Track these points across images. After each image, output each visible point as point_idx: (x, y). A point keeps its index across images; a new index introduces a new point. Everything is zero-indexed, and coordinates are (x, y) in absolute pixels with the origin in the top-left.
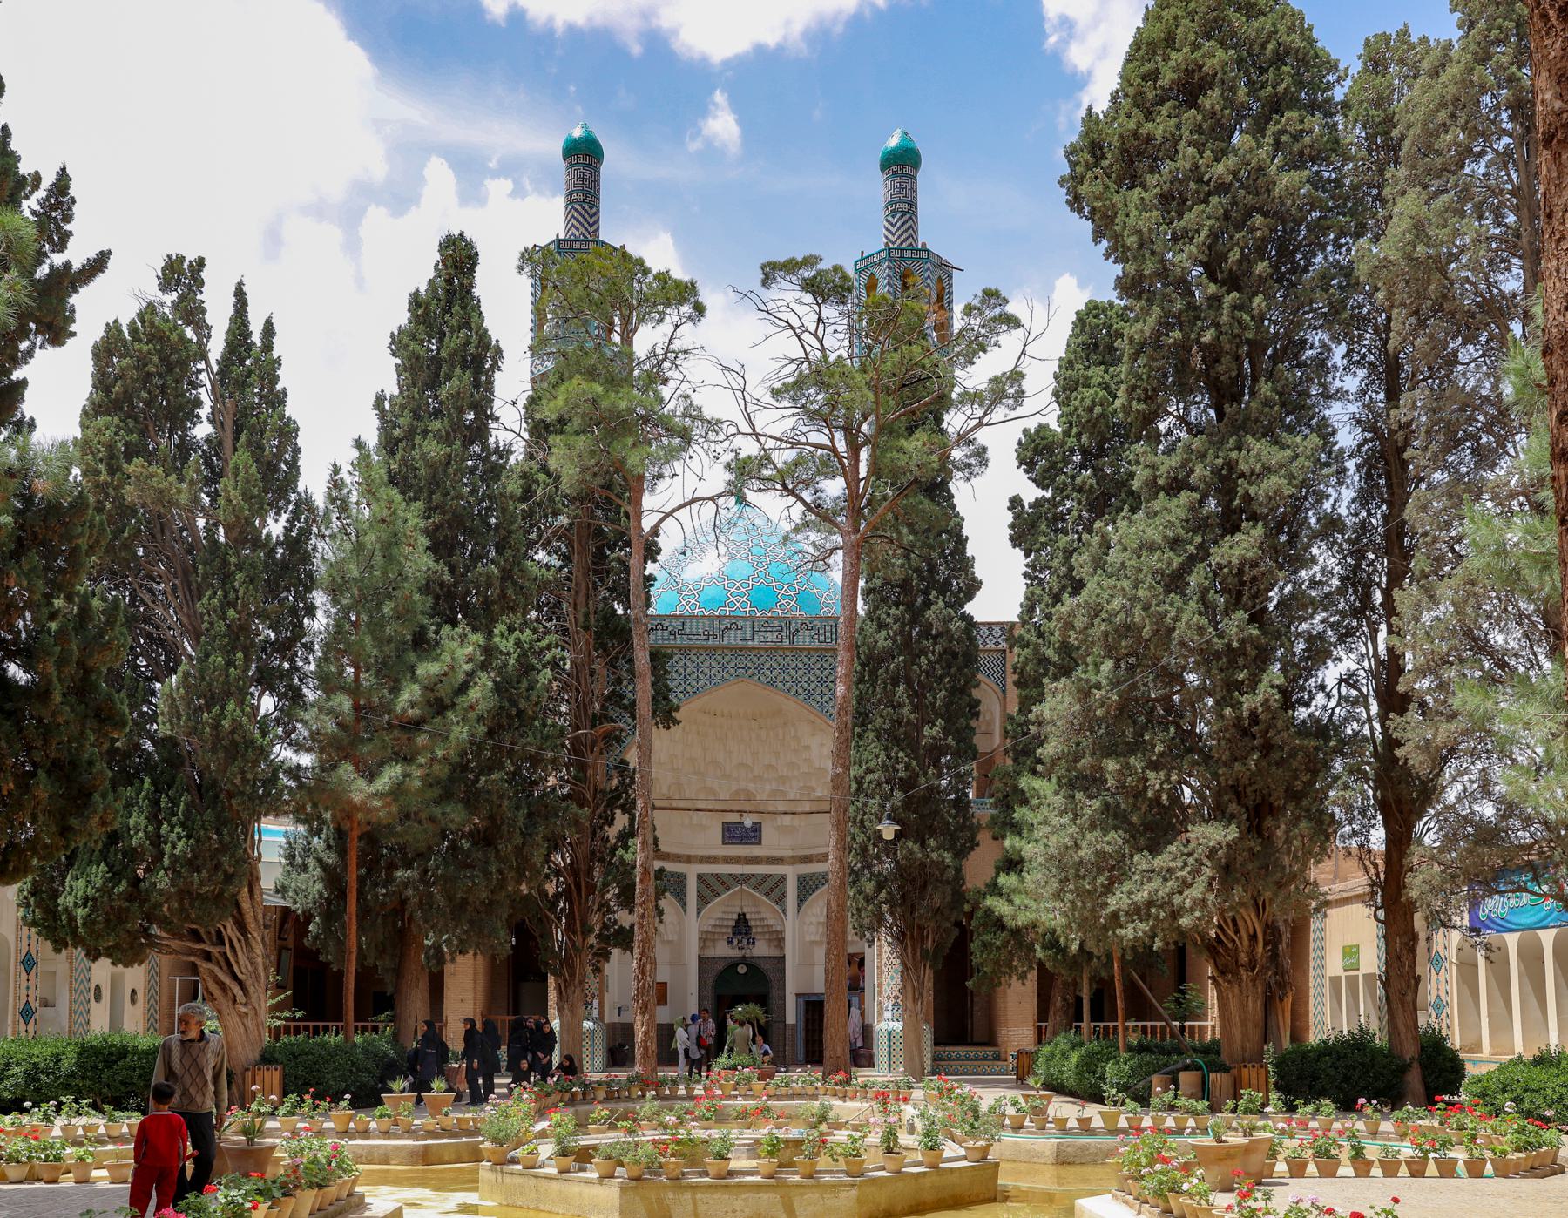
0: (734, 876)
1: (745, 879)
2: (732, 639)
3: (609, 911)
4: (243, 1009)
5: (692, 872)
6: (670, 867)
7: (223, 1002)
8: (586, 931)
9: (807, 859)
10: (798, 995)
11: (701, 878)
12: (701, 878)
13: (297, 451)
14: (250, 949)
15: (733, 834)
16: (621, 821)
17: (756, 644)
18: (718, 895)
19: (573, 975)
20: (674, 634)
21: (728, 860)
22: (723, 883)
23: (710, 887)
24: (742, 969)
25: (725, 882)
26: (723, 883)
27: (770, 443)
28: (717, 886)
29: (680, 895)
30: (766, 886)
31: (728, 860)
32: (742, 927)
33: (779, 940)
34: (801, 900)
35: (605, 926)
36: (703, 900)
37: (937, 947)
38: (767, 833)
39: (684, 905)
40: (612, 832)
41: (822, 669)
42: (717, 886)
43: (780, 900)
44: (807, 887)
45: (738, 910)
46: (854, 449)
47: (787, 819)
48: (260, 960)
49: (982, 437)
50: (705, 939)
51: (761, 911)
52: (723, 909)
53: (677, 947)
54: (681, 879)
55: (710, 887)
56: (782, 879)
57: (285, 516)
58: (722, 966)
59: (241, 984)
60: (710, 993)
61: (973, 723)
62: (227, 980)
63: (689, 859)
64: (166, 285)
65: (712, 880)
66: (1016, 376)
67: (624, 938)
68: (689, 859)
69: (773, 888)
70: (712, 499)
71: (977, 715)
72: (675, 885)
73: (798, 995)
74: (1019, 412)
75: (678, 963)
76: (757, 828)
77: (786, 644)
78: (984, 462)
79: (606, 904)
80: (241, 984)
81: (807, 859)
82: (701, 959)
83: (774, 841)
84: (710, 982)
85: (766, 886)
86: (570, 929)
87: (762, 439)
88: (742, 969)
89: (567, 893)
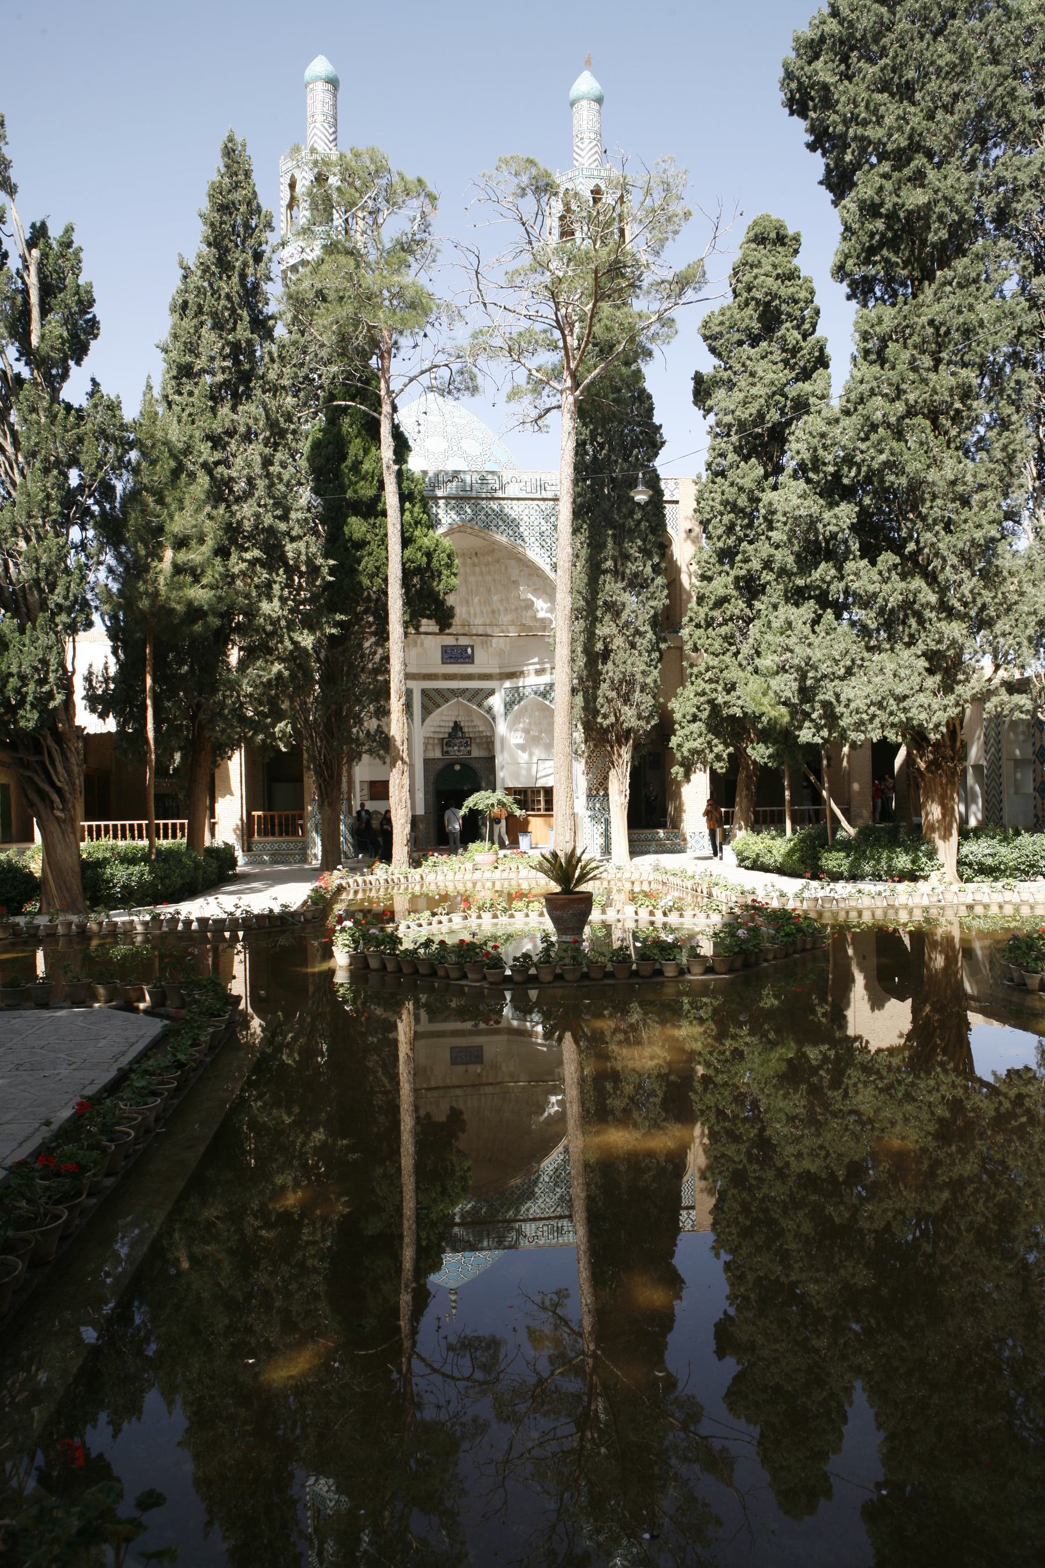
0: (452, 691)
1: (463, 692)
4: (59, 814)
11: (424, 692)
14: (66, 759)
18: (439, 706)
22: (443, 696)
24: (457, 767)
26: (443, 696)
28: (439, 700)
36: (426, 711)
38: (480, 655)
42: (439, 700)
45: (453, 719)
48: (76, 769)
58: (440, 766)
59: (59, 791)
62: (47, 788)
65: (433, 694)
80: (59, 791)
82: (427, 761)
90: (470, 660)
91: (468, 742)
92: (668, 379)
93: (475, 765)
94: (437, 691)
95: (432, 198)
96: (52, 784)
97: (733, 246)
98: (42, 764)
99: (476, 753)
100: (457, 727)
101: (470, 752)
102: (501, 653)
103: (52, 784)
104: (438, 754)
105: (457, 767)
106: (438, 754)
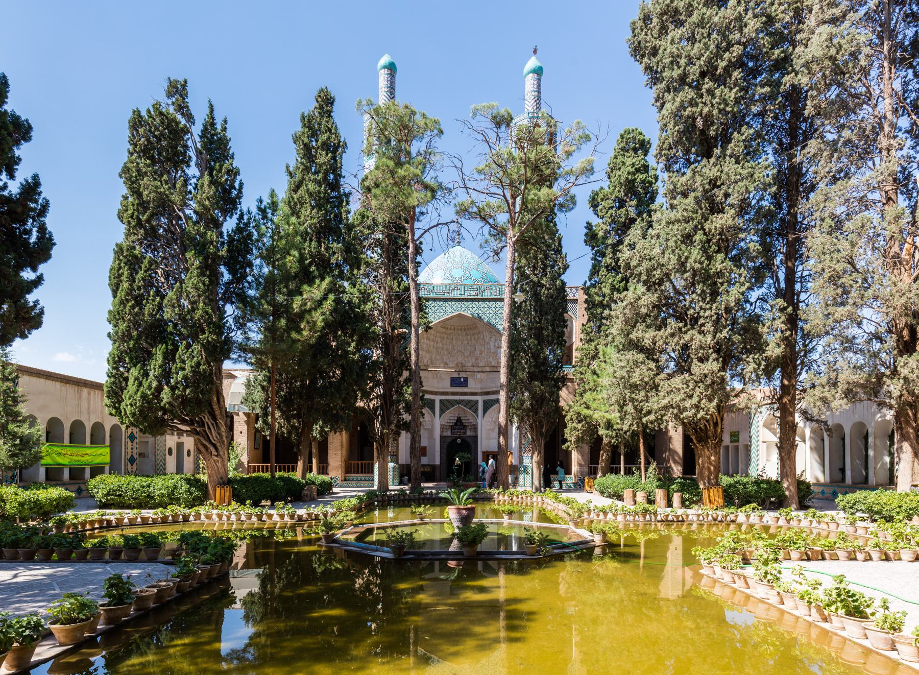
0: (456, 401)
1: (461, 402)
2: (456, 294)
3: (400, 414)
5: (437, 399)
6: (427, 396)
7: (207, 455)
8: (390, 423)
9: (487, 393)
10: (483, 453)
11: (441, 401)
12: (441, 401)
13: (241, 184)
15: (455, 382)
16: (406, 374)
17: (466, 296)
19: (383, 443)
20: (429, 291)
21: (453, 394)
23: (445, 406)
25: (452, 403)
27: (474, 195)
29: (432, 408)
30: (470, 405)
31: (453, 394)
32: (459, 423)
33: (475, 428)
34: (485, 411)
35: (399, 421)
36: (442, 411)
37: (547, 431)
38: (471, 383)
39: (434, 413)
40: (402, 379)
41: (496, 308)
43: (476, 411)
44: (488, 405)
46: (514, 197)
47: (479, 375)
49: (574, 190)
50: (443, 428)
51: (468, 416)
52: (450, 415)
53: (431, 431)
54: (433, 401)
55: (445, 406)
56: (477, 402)
57: (235, 217)
58: (449, 440)
60: (445, 451)
61: (565, 330)
63: (436, 393)
64: (170, 95)
66: (591, 163)
67: (406, 426)
68: (436, 393)
69: (473, 406)
70: (446, 224)
71: (566, 327)
72: (431, 405)
73: (483, 453)
74: (592, 178)
75: (431, 438)
76: (466, 379)
77: (479, 296)
78: (574, 203)
79: (399, 411)
81: (487, 393)
82: (442, 437)
83: (473, 386)
84: (445, 446)
85: (470, 405)
86: (382, 423)
87: (470, 191)
88: (459, 441)
89: (381, 407)
90: (465, 383)
91: (465, 428)
92: (572, 227)
93: (469, 440)
94: (448, 400)
95: (441, 132)
96: (211, 442)
97: (610, 146)
98: (205, 431)
99: (469, 433)
100: (459, 420)
101: (465, 433)
102: (481, 381)
103: (211, 442)
104: (449, 433)
105: (459, 441)
106: (449, 433)
